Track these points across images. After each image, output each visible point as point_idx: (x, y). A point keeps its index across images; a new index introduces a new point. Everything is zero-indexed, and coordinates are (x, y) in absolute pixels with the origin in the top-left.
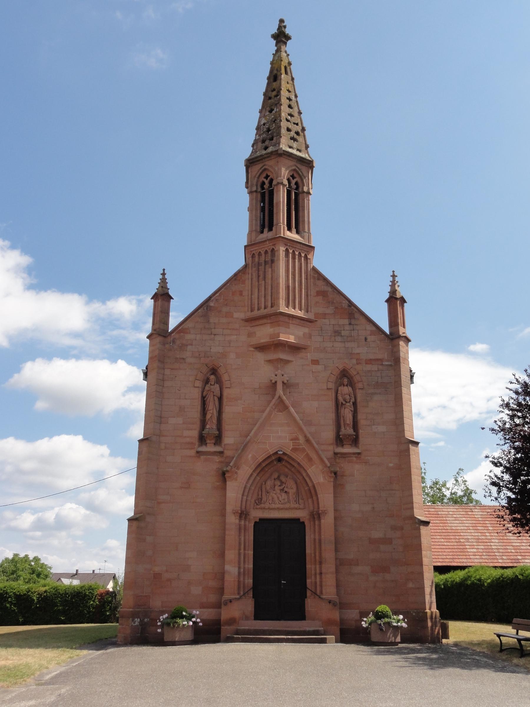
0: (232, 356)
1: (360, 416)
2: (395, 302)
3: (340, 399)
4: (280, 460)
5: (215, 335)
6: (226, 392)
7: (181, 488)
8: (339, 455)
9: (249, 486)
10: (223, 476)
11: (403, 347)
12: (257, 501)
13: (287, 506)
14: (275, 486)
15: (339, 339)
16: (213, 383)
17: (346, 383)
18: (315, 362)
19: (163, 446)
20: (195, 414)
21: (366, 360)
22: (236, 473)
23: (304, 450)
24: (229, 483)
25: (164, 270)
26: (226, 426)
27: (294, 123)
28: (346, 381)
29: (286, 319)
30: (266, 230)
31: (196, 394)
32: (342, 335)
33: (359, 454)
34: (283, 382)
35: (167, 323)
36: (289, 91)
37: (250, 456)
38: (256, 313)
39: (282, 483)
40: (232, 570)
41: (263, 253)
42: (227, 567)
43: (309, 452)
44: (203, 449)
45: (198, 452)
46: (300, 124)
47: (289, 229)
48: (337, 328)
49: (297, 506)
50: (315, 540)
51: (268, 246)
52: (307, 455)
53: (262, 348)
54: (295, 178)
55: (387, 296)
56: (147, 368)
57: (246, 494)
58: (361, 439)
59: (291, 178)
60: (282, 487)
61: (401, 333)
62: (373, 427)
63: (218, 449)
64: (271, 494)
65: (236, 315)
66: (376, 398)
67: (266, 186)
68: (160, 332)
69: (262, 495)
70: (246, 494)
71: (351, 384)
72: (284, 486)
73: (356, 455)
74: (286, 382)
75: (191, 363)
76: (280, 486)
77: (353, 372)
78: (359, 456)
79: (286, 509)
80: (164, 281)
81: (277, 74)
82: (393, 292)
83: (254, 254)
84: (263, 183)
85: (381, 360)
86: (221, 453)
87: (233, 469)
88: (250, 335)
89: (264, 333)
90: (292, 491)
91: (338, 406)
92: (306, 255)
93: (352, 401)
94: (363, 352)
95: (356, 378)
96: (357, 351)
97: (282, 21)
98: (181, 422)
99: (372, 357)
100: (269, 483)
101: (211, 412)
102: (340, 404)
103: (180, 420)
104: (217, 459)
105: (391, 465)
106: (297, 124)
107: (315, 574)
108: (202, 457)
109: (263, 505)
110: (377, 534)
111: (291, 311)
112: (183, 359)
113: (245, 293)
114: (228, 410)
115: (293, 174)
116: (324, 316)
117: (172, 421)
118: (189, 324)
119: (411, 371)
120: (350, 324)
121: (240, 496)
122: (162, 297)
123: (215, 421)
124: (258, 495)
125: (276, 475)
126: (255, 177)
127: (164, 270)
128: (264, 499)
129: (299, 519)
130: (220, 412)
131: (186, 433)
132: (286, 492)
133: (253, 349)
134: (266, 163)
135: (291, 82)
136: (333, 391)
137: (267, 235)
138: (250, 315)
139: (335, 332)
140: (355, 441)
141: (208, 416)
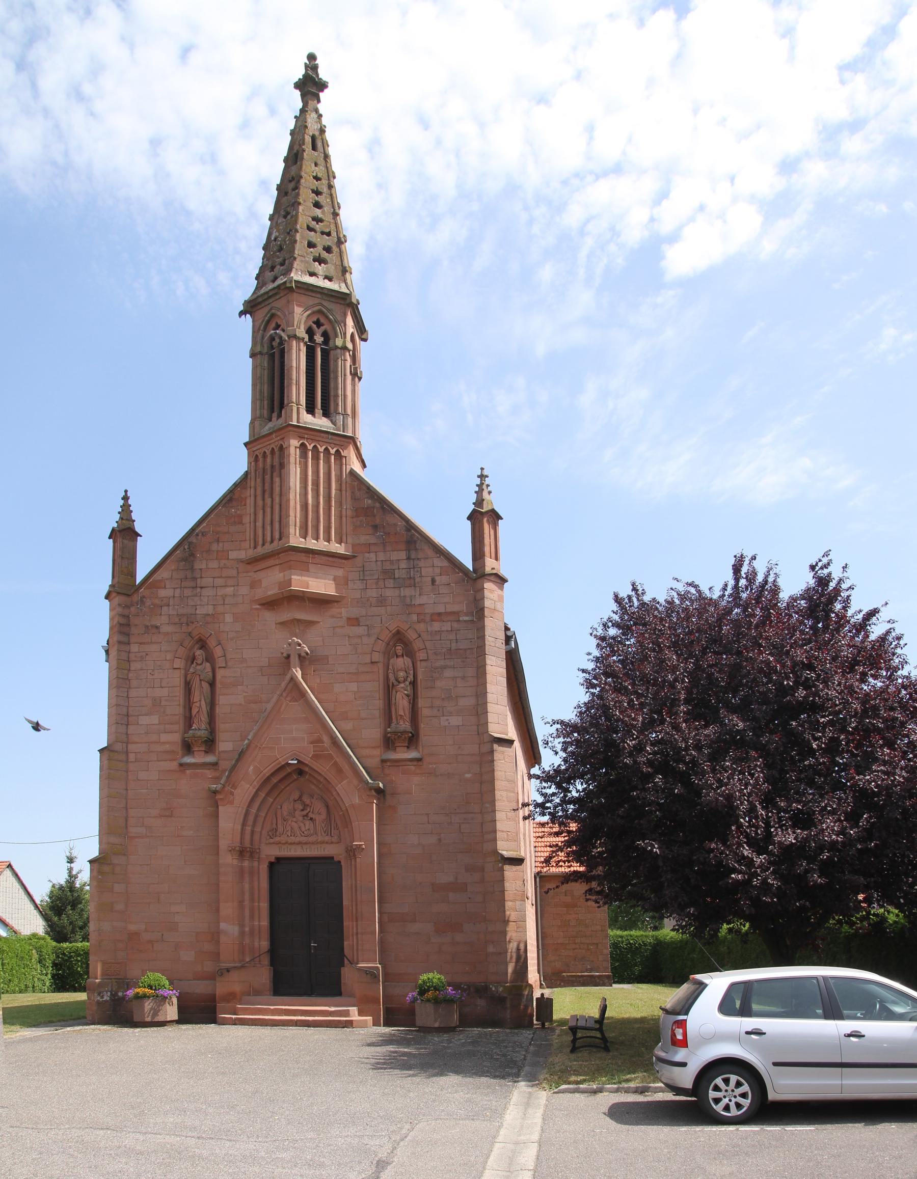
0: (228, 618)
1: (421, 703)
2: (483, 518)
3: (391, 676)
5: (201, 588)
6: (220, 674)
7: (161, 816)
8: (388, 764)
9: (253, 811)
10: (214, 798)
13: (311, 839)
15: (390, 583)
16: (199, 662)
17: (400, 652)
18: (354, 621)
19: (132, 757)
20: (176, 709)
21: (432, 614)
22: (232, 793)
23: (330, 757)
24: (221, 809)
25: (126, 491)
26: (221, 726)
27: (323, 233)
28: (399, 649)
29: (302, 557)
31: (177, 679)
32: (397, 576)
33: (419, 760)
34: (299, 656)
35: (133, 575)
36: (317, 178)
37: (251, 768)
38: (260, 551)
39: (305, 806)
40: (229, 929)
41: (268, 453)
42: (223, 926)
43: (338, 760)
44: (188, 760)
45: (181, 765)
46: (334, 234)
47: (311, 410)
48: (388, 566)
49: (327, 838)
51: (274, 442)
52: (336, 764)
53: (271, 604)
54: (323, 325)
57: (250, 822)
58: (423, 738)
59: (315, 326)
60: (305, 813)
61: (488, 570)
63: (210, 759)
65: (233, 555)
66: (448, 673)
68: (124, 589)
70: (250, 822)
71: (409, 653)
73: (415, 763)
75: (168, 633)
76: (302, 810)
77: (411, 635)
78: (420, 763)
80: (126, 510)
82: (479, 502)
83: (257, 456)
85: (456, 613)
86: (215, 764)
87: (227, 788)
88: (253, 585)
89: (270, 581)
90: (321, 817)
91: (389, 689)
92: (338, 452)
93: (409, 679)
94: (428, 601)
95: (418, 644)
96: (418, 601)
98: (157, 722)
99: (441, 609)
100: (287, 807)
101: (198, 704)
103: (155, 719)
104: (209, 773)
105: (468, 776)
106: (329, 234)
109: (277, 839)
110: (444, 878)
111: (311, 544)
112: (157, 627)
113: (246, 520)
114: (223, 701)
115: (318, 320)
118: (163, 574)
119: (507, 629)
120: (409, 558)
121: (239, 827)
122: (125, 534)
123: (204, 717)
125: (296, 795)
126: (259, 329)
127: (126, 491)
128: (280, 829)
129: (332, 858)
130: (212, 704)
131: (164, 737)
134: (273, 305)
135: (321, 161)
136: (381, 665)
137: (275, 423)
138: (251, 553)
139: (385, 572)
140: (412, 740)
141: (194, 711)
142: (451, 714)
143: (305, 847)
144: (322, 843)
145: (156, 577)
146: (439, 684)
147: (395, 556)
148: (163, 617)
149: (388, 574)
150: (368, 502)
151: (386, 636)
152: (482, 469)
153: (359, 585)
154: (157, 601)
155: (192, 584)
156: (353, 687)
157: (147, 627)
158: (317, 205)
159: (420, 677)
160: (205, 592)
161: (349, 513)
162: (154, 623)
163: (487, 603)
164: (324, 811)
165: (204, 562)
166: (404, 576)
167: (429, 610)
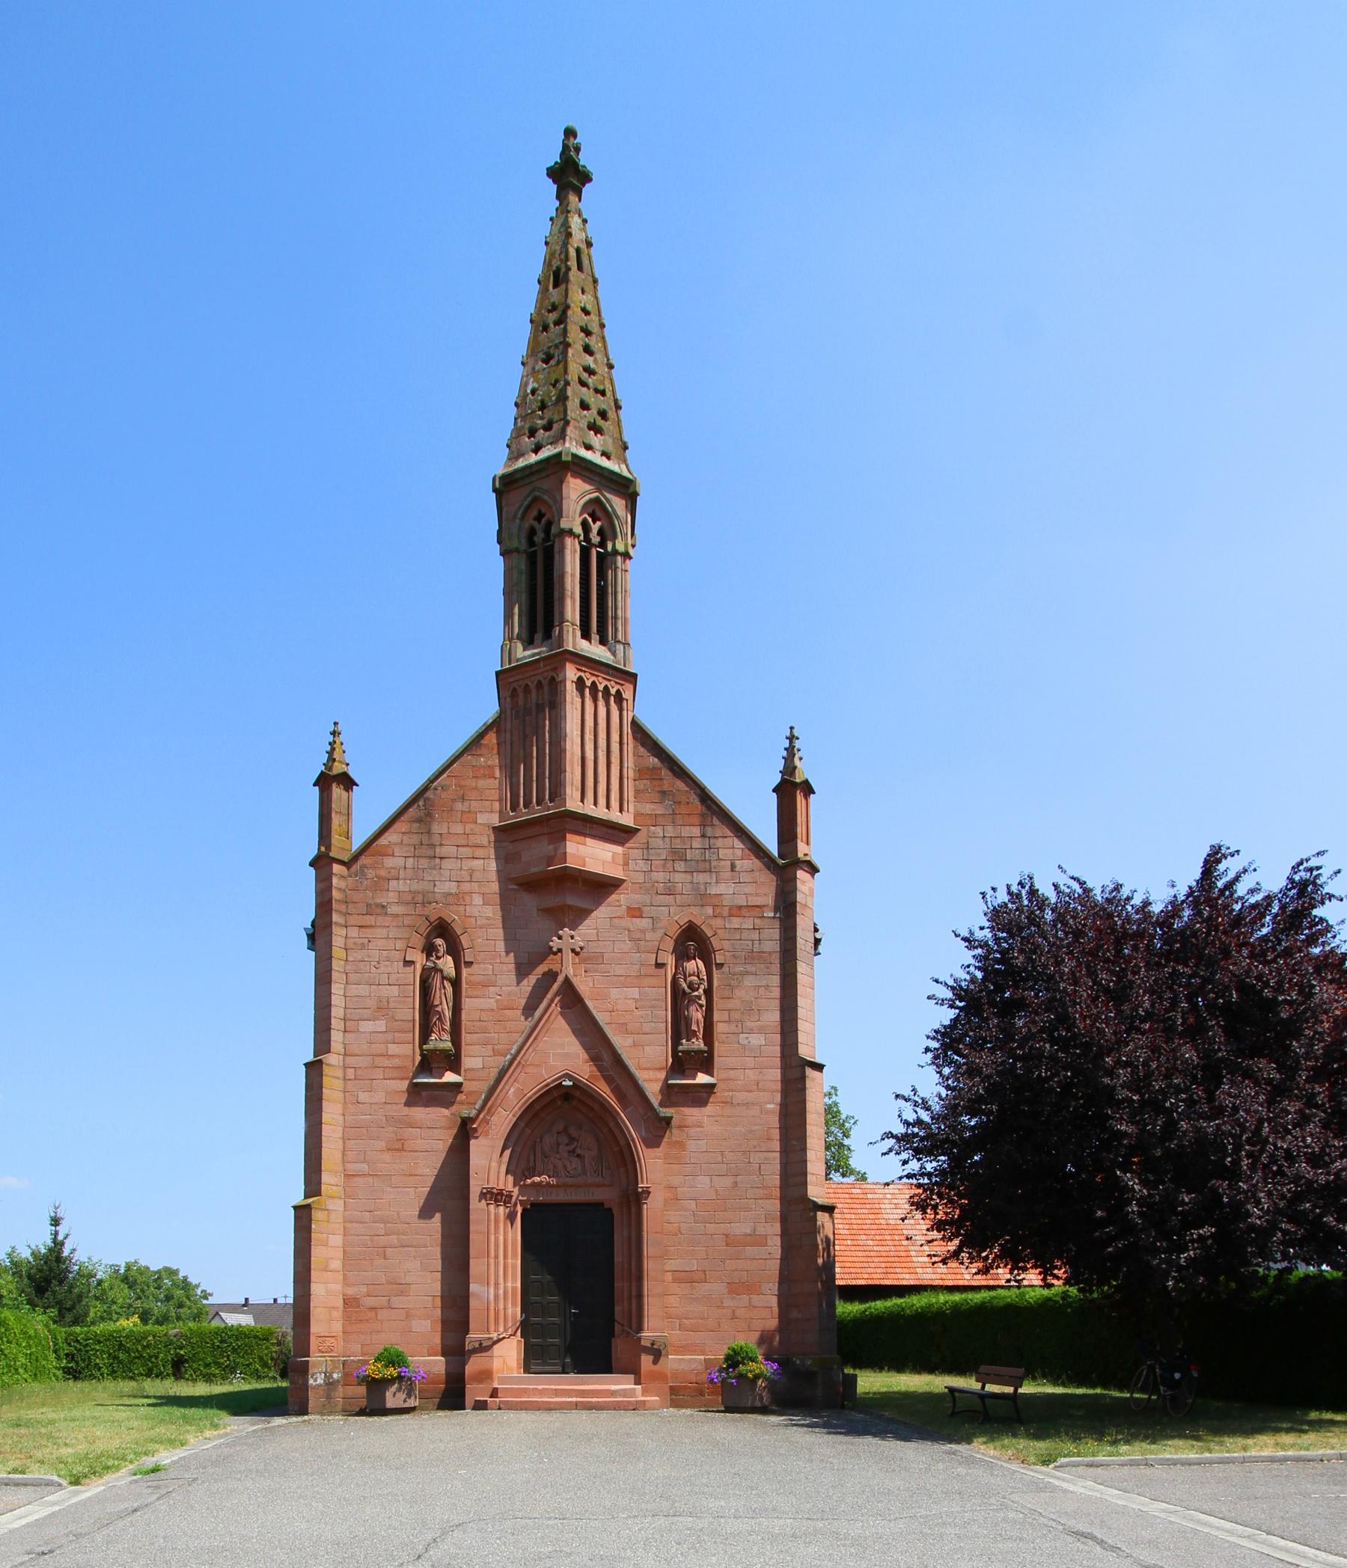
1: (716, 1016)
2: (791, 791)
11: (804, 882)
15: (680, 866)
18: (635, 912)
20: (410, 1011)
21: (731, 908)
27: (597, 391)
30: (538, 636)
34: (573, 951)
36: (586, 312)
39: (572, 1139)
41: (532, 686)
46: (609, 394)
47: (586, 635)
48: (678, 844)
50: (630, 1238)
55: (777, 779)
58: (717, 1061)
60: (571, 1148)
61: (800, 855)
65: (481, 819)
66: (749, 981)
67: (539, 537)
75: (397, 915)
81: (562, 268)
82: (789, 769)
83: (515, 690)
84: (532, 532)
97: (570, 133)
100: (549, 1140)
103: (381, 1025)
106: (603, 393)
107: (630, 1298)
111: (589, 809)
116: (655, 820)
117: (367, 1026)
120: (703, 836)
122: (333, 781)
125: (560, 1127)
126: (515, 517)
130: (457, 1009)
131: (393, 1049)
135: (589, 287)
140: (706, 1062)
142: (751, 1031)
145: (383, 841)
146: (738, 993)
147: (686, 831)
148: (391, 894)
149: (678, 855)
150: (654, 761)
151: (675, 931)
152: (792, 728)
153: (642, 865)
154: (383, 873)
156: (634, 993)
157: (368, 905)
158: (588, 350)
159: (715, 983)
160: (446, 864)
161: (631, 774)
162: (378, 901)
163: (800, 897)
165: (445, 825)
166: (698, 858)
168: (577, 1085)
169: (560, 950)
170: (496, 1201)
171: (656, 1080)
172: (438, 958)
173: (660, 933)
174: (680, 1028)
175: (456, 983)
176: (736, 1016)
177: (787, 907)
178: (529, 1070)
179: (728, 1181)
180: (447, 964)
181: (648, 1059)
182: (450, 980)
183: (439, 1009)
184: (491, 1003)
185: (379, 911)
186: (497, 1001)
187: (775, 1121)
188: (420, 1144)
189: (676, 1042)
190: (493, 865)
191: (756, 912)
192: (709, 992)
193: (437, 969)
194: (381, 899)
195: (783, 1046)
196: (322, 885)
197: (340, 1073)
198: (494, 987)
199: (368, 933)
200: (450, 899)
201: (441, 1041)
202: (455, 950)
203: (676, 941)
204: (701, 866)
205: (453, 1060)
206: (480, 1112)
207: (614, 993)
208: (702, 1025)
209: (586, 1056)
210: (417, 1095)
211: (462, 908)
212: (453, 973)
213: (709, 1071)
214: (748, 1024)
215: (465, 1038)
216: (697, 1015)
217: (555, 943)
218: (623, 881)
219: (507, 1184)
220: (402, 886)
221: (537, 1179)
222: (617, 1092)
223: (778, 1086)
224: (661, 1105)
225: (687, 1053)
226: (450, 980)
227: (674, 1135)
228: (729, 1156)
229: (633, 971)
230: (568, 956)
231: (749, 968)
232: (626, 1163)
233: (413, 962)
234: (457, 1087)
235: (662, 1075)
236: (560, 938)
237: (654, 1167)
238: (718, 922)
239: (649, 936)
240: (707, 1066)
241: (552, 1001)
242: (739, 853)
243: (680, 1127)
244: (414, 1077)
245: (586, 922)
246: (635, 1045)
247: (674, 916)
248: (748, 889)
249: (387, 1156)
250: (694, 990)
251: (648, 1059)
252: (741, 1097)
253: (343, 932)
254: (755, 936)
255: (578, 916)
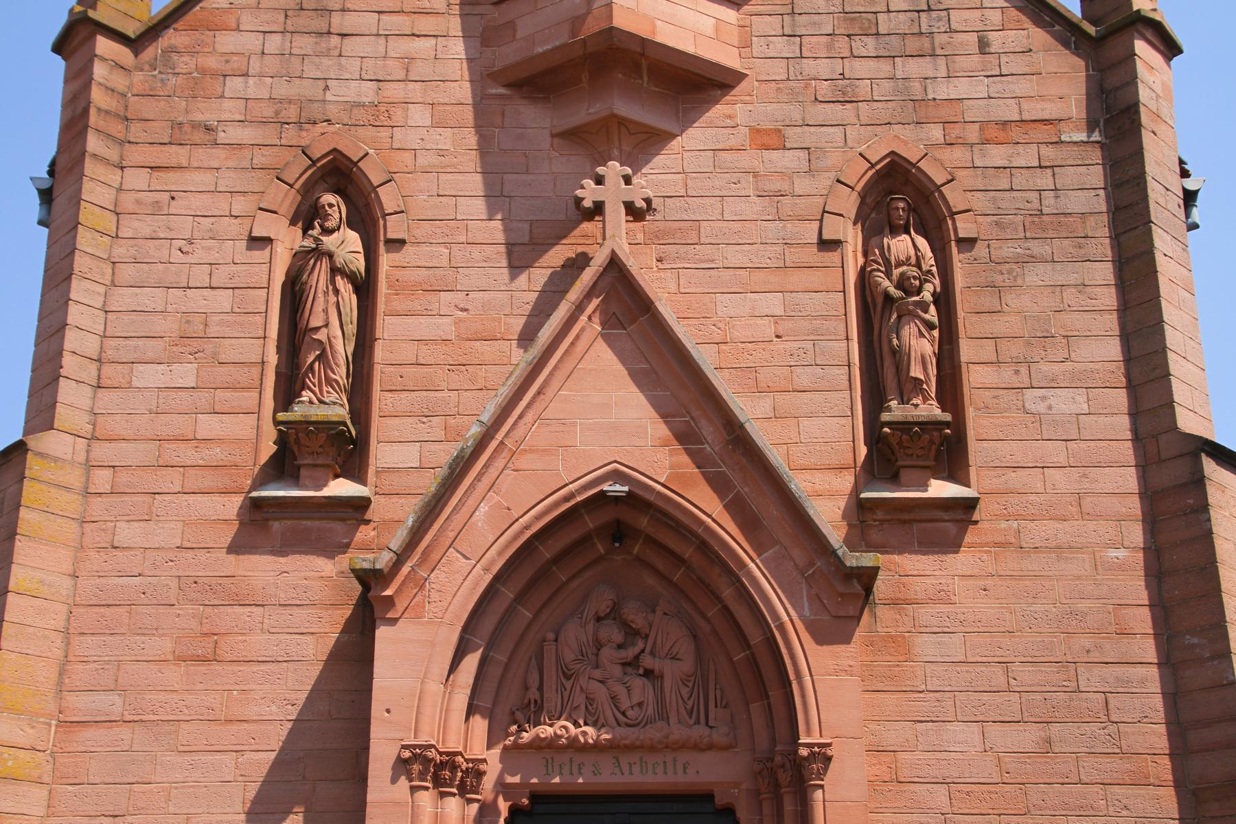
1: (967, 351)
4: (619, 533)
5: (343, 35)
7: (181, 659)
8: (880, 515)
12: (519, 716)
13: (653, 733)
14: (599, 646)
15: (868, 45)
18: (769, 138)
21: (983, 125)
39: (632, 633)
56: (51, 173)
60: (630, 653)
62: (1029, 393)
64: (583, 681)
66: (1036, 276)
69: (540, 688)
72: (640, 644)
74: (640, 204)
76: (620, 646)
79: (652, 748)
96: (943, 91)
100: (575, 635)
102: (880, 300)
103: (186, 374)
108: (276, 526)
112: (208, 129)
124: (527, 688)
125: (602, 601)
129: (708, 797)
131: (209, 426)
132: (648, 673)
133: (502, 91)
140: (949, 452)
142: (1053, 384)
143: (625, 760)
144: (681, 746)
148: (227, 104)
151: (859, 174)
153: (781, 46)
154: (212, 62)
155: (320, 24)
156: (774, 304)
162: (199, 117)
163: (1144, 94)
164: (686, 649)
166: (904, 29)
167: (975, 112)
168: (638, 501)
169: (599, 208)
170: (438, 782)
171: (832, 495)
172: (328, 232)
173: (826, 180)
174: (880, 373)
175: (365, 287)
176: (1013, 349)
177: (1116, 120)
178: (522, 462)
179: (1028, 737)
180: (347, 245)
181: (815, 443)
182: (351, 277)
183: (321, 336)
184: (445, 327)
185: (199, 136)
186: (458, 322)
187: (1137, 589)
188: (259, 644)
189: (874, 398)
190: (458, 48)
191: (1042, 133)
192: (945, 301)
193: (318, 253)
194: (205, 113)
195: (1135, 413)
196: (76, 85)
197: (74, 478)
198: (452, 290)
199: (172, 180)
200: (359, 114)
201: (324, 404)
202: (365, 218)
203: (863, 196)
204: (913, 45)
205: (348, 448)
206: (401, 558)
207: (727, 305)
208: (933, 371)
209: (663, 430)
210: (261, 526)
211: (385, 133)
212: (359, 264)
213: (957, 473)
214: (1044, 367)
215: (380, 400)
216: (920, 346)
217: (589, 193)
218: (739, 77)
219: (471, 739)
220: (253, 88)
221: (545, 731)
222: (737, 508)
223: (1134, 506)
224: (848, 542)
225: (903, 426)
226: (351, 277)
227: (880, 620)
228: (1026, 675)
229: (768, 256)
230: (616, 215)
231: (1037, 248)
232: (767, 683)
233: (267, 241)
234: (359, 506)
235: (846, 482)
236: (599, 180)
237: (834, 690)
238: (958, 155)
239: (802, 185)
240: (955, 468)
241: (579, 308)
242: (995, 17)
243: (895, 603)
244: (254, 487)
245: (659, 160)
246: (777, 416)
247: (855, 147)
248: (1022, 87)
249: (174, 675)
250: (908, 293)
251: (815, 443)
252: (1037, 532)
253: (114, 177)
254: (1045, 180)
255: (644, 143)
